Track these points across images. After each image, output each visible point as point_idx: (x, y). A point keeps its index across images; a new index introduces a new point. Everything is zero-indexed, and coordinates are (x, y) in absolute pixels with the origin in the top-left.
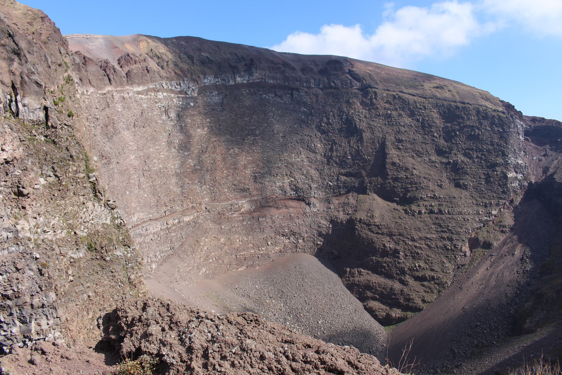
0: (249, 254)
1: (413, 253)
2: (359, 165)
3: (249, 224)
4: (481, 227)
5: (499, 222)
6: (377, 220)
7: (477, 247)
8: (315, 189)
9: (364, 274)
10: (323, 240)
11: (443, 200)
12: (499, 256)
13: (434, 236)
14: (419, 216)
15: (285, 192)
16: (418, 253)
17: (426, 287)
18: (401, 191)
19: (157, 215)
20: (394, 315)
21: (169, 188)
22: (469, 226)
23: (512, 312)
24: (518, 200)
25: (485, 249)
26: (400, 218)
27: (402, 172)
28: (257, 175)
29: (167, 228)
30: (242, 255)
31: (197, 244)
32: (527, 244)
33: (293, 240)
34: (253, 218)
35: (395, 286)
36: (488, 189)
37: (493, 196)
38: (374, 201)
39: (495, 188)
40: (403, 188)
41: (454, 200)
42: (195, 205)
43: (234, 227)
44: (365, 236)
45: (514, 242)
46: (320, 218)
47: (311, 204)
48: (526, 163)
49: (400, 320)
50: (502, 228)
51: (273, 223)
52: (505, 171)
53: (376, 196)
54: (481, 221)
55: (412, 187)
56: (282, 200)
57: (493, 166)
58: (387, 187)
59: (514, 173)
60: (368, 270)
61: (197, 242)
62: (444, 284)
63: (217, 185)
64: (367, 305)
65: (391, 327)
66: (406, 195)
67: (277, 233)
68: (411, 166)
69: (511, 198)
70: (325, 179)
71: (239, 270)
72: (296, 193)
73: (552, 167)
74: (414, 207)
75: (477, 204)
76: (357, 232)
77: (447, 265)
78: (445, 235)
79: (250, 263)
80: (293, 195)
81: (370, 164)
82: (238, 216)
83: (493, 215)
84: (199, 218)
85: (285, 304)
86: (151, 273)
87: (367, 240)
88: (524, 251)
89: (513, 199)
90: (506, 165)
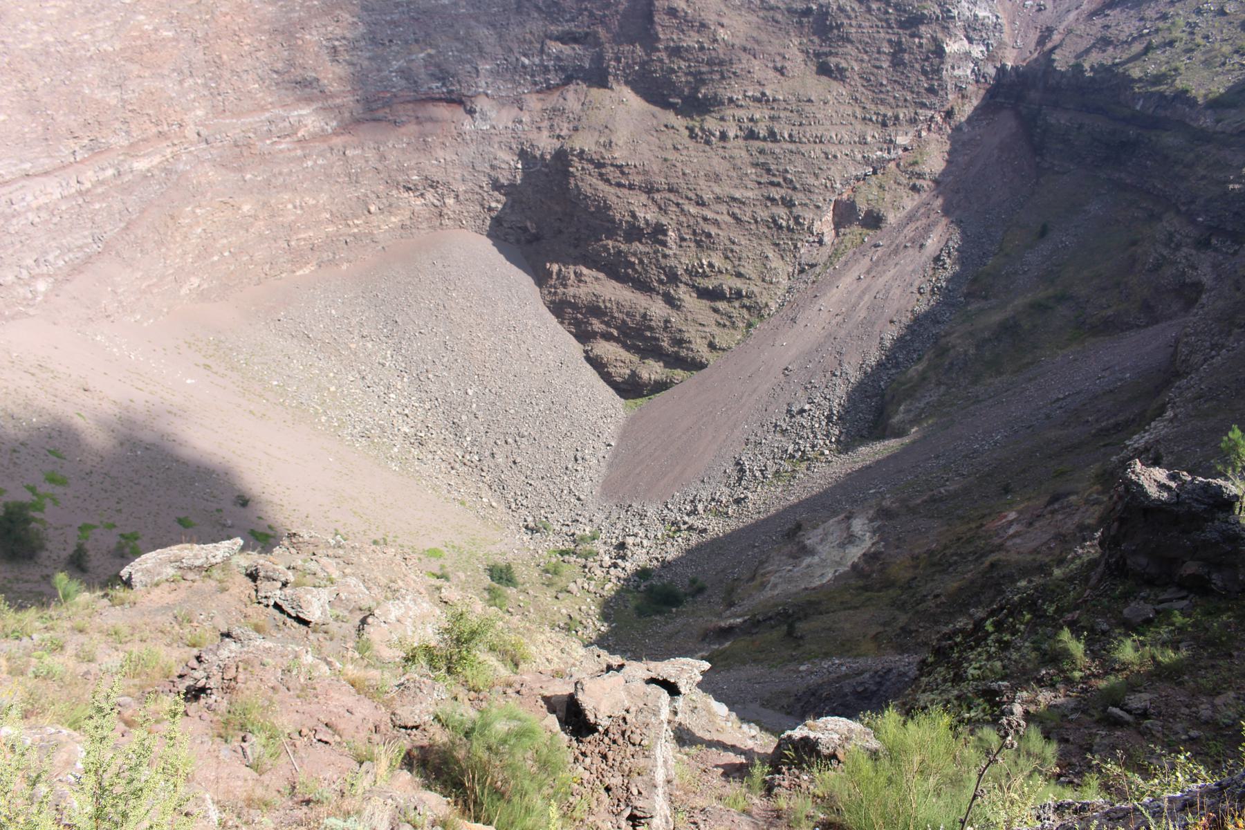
0: (323, 236)
1: (699, 234)
2: (591, 15)
3: (321, 166)
4: (866, 175)
5: (911, 165)
6: (620, 155)
7: (851, 223)
8: (487, 74)
9: (588, 280)
10: (503, 199)
11: (783, 105)
12: (892, 248)
13: (750, 194)
14: (721, 144)
15: (415, 82)
16: (709, 235)
17: (722, 314)
18: (686, 82)
19: (46, 163)
20: (647, 376)
21: (78, 93)
22: (835, 172)
23: (882, 383)
24: (965, 111)
25: (868, 229)
26: (675, 148)
27: (692, 33)
28: (337, 43)
29: (80, 193)
30: (305, 239)
31: (170, 223)
32: (959, 223)
33: (432, 199)
34: (332, 149)
35: (653, 309)
36: (895, 81)
37: (906, 100)
38: (622, 106)
39: (913, 81)
40: (690, 73)
41: (808, 108)
42: (166, 128)
43: (280, 174)
44: (589, 192)
45: (933, 216)
46: (496, 146)
47: (475, 112)
48: (997, 17)
49: (661, 386)
50: (914, 180)
51: (380, 161)
52: (940, 35)
53: (627, 93)
54: (866, 161)
55: (711, 72)
56: (409, 102)
57: (913, 22)
58: (655, 71)
59: (965, 42)
60: (599, 270)
61: (172, 217)
62: (761, 309)
63: (227, 75)
64: (591, 350)
65: (639, 401)
66: (697, 90)
67: (392, 183)
68: (713, 17)
69: (948, 107)
70: (511, 50)
71: (298, 274)
72: (444, 85)
73: (1061, 28)
74: (711, 123)
75: (864, 119)
76: (572, 181)
77: (775, 262)
78: (776, 193)
79: (325, 256)
80: (435, 91)
81: (617, 12)
82: (291, 146)
83: (900, 146)
84: (178, 160)
85: (397, 350)
86: (31, 303)
87: (595, 200)
88: (948, 240)
89: (952, 108)
90: (945, 20)
